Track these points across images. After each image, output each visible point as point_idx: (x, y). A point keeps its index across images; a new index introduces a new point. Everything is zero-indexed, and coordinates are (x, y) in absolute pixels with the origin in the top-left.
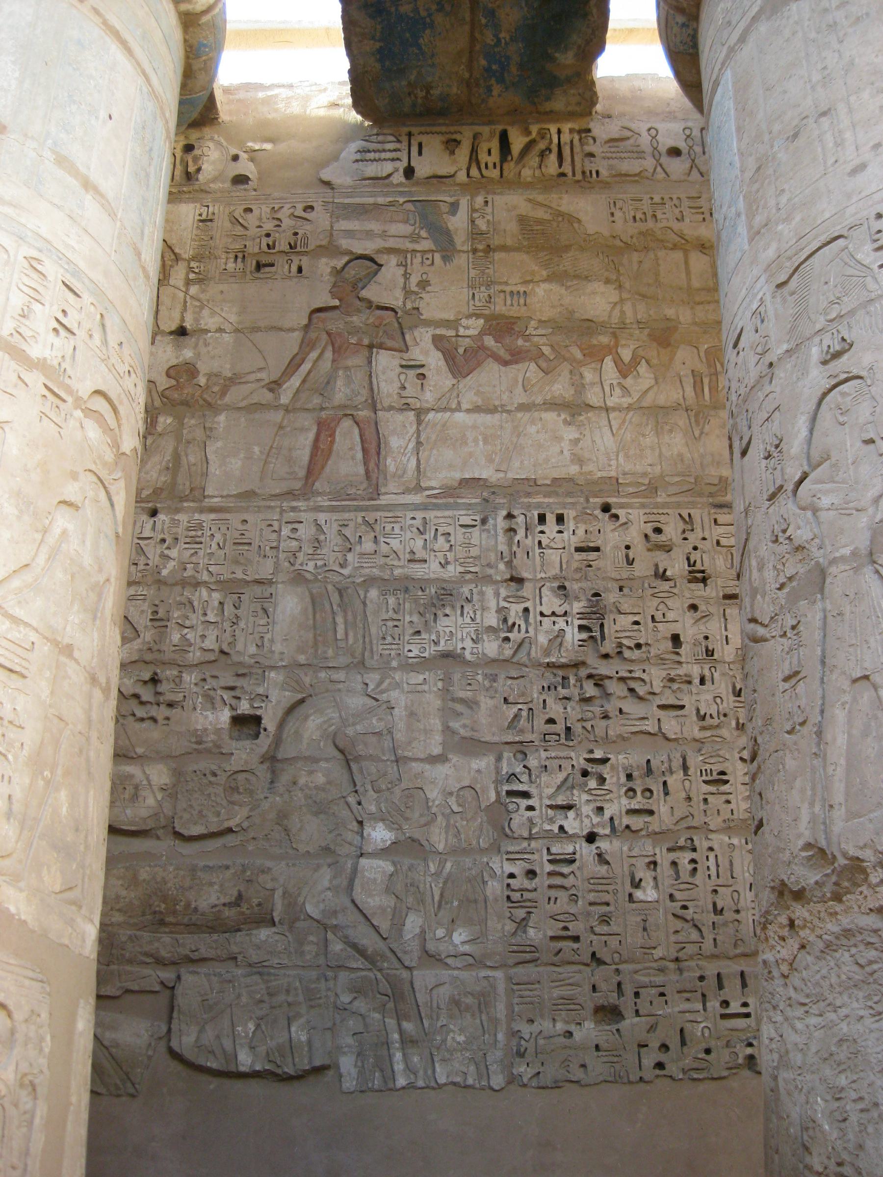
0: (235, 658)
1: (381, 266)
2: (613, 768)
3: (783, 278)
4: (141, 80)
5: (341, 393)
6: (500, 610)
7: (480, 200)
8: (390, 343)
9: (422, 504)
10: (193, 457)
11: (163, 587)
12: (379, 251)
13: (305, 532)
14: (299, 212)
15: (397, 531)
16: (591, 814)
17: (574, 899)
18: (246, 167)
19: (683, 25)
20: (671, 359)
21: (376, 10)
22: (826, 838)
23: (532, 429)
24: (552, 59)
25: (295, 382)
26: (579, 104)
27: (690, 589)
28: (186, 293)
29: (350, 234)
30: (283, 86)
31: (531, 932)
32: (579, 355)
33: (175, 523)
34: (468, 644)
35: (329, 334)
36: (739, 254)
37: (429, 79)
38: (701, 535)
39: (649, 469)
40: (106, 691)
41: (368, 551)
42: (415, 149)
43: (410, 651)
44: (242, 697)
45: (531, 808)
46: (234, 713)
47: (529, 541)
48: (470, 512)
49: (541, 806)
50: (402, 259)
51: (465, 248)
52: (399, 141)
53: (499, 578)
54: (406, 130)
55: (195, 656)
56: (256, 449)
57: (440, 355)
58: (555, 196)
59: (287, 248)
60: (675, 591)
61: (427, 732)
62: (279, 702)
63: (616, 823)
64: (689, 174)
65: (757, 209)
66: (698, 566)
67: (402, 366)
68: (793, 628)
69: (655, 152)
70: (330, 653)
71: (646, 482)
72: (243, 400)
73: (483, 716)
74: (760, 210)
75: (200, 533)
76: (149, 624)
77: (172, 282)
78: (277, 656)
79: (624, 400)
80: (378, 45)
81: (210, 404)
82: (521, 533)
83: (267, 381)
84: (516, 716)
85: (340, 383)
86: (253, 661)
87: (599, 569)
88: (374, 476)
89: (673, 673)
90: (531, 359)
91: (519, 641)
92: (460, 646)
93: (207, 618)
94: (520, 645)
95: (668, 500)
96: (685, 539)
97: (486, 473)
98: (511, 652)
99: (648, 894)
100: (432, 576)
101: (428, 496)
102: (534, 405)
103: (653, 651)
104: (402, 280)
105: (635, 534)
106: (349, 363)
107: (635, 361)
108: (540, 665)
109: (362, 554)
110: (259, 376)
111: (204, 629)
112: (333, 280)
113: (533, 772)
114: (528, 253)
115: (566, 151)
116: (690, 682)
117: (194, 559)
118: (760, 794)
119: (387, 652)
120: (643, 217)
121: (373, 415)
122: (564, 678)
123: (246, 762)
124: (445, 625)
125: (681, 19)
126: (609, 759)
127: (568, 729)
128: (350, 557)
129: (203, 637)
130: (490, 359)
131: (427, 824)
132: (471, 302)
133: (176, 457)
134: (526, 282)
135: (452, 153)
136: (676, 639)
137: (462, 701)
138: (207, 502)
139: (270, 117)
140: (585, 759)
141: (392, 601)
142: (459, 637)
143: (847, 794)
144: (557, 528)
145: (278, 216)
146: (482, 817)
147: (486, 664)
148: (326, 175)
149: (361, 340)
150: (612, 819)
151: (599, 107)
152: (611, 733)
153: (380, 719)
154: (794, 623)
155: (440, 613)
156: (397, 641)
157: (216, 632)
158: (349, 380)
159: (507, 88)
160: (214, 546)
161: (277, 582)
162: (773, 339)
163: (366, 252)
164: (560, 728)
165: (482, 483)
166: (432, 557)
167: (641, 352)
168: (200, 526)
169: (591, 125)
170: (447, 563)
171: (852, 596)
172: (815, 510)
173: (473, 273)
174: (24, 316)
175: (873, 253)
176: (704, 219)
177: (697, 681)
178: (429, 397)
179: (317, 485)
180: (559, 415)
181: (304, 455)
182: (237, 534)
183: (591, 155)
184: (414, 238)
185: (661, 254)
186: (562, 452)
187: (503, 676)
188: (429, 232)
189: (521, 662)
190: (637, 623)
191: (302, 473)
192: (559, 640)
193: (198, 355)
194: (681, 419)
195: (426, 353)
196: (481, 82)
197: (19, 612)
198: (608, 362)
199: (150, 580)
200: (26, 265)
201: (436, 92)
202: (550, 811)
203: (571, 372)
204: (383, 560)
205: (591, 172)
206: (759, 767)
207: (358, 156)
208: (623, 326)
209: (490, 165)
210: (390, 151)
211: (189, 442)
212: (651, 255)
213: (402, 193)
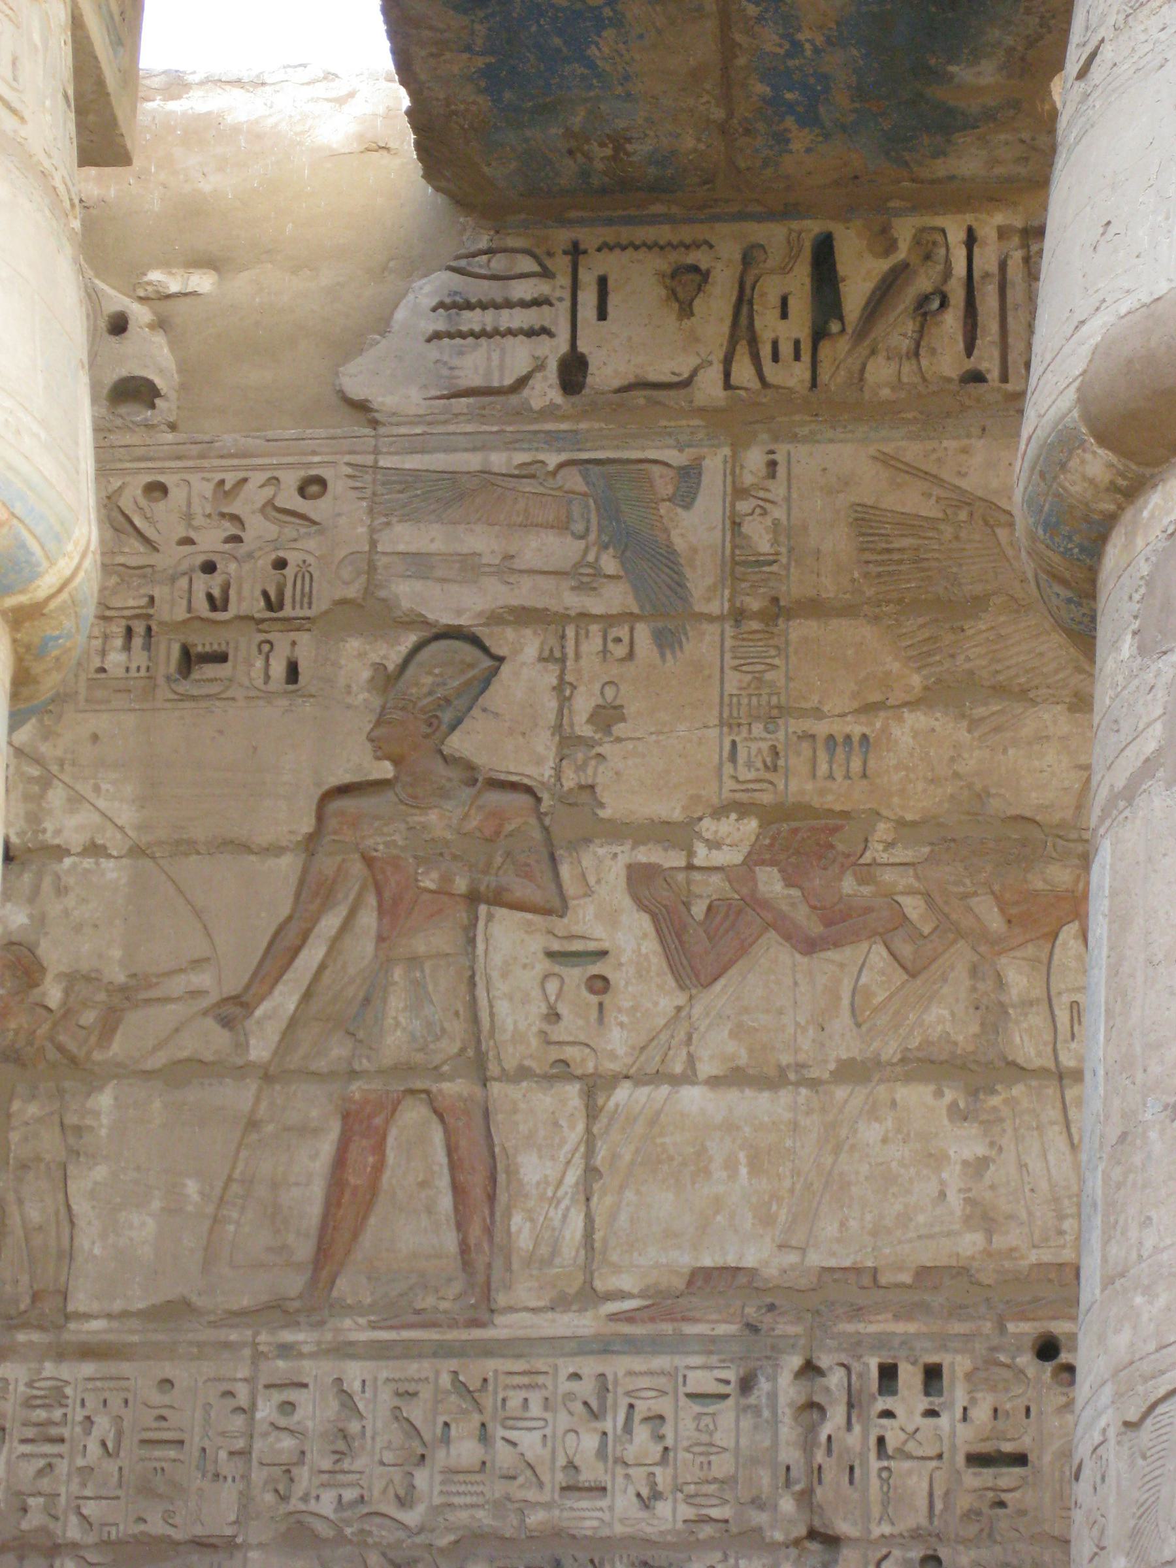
1: (501, 660)
7: (755, 459)
8: (521, 890)
9: (597, 1337)
12: (495, 618)
14: (290, 499)
15: (535, 1409)
23: (870, 1133)
30: (238, 83)
32: (995, 922)
35: (369, 861)
37: (621, 124)
42: (588, 299)
47: (853, 1440)
48: (713, 1360)
50: (553, 641)
51: (714, 608)
52: (546, 274)
53: (779, 1536)
54: (563, 236)
56: (192, 1188)
57: (645, 922)
58: (951, 444)
59: (258, 607)
67: (551, 955)
72: (157, 1048)
75: (57, 1414)
80: (480, 62)
81: (73, 1060)
85: (396, 1003)
87: (1022, 1513)
88: (480, 1261)
100: (619, 1529)
101: (613, 1317)
102: (878, 1064)
104: (554, 704)
109: (451, 1472)
112: (376, 702)
114: (876, 618)
115: (988, 302)
117: (45, 1484)
121: (478, 1090)
128: (421, 1478)
130: (772, 934)
132: (728, 769)
134: (870, 709)
135: (686, 310)
138: (79, 1331)
139: (206, 186)
144: (923, 1403)
145: (235, 508)
149: (447, 879)
160: (94, 1449)
161: (244, 1546)
163: (462, 621)
165: (742, 1280)
166: (620, 1480)
168: (57, 1397)
170: (656, 1495)
179: (343, 1285)
180: (939, 1094)
186: (943, 1195)
188: (622, 558)
191: (304, 1250)
195: (612, 918)
201: (640, 149)
203: (974, 971)
204: (499, 1489)
209: (786, 349)
210: (524, 304)
211: (24, 1167)
213: (553, 440)
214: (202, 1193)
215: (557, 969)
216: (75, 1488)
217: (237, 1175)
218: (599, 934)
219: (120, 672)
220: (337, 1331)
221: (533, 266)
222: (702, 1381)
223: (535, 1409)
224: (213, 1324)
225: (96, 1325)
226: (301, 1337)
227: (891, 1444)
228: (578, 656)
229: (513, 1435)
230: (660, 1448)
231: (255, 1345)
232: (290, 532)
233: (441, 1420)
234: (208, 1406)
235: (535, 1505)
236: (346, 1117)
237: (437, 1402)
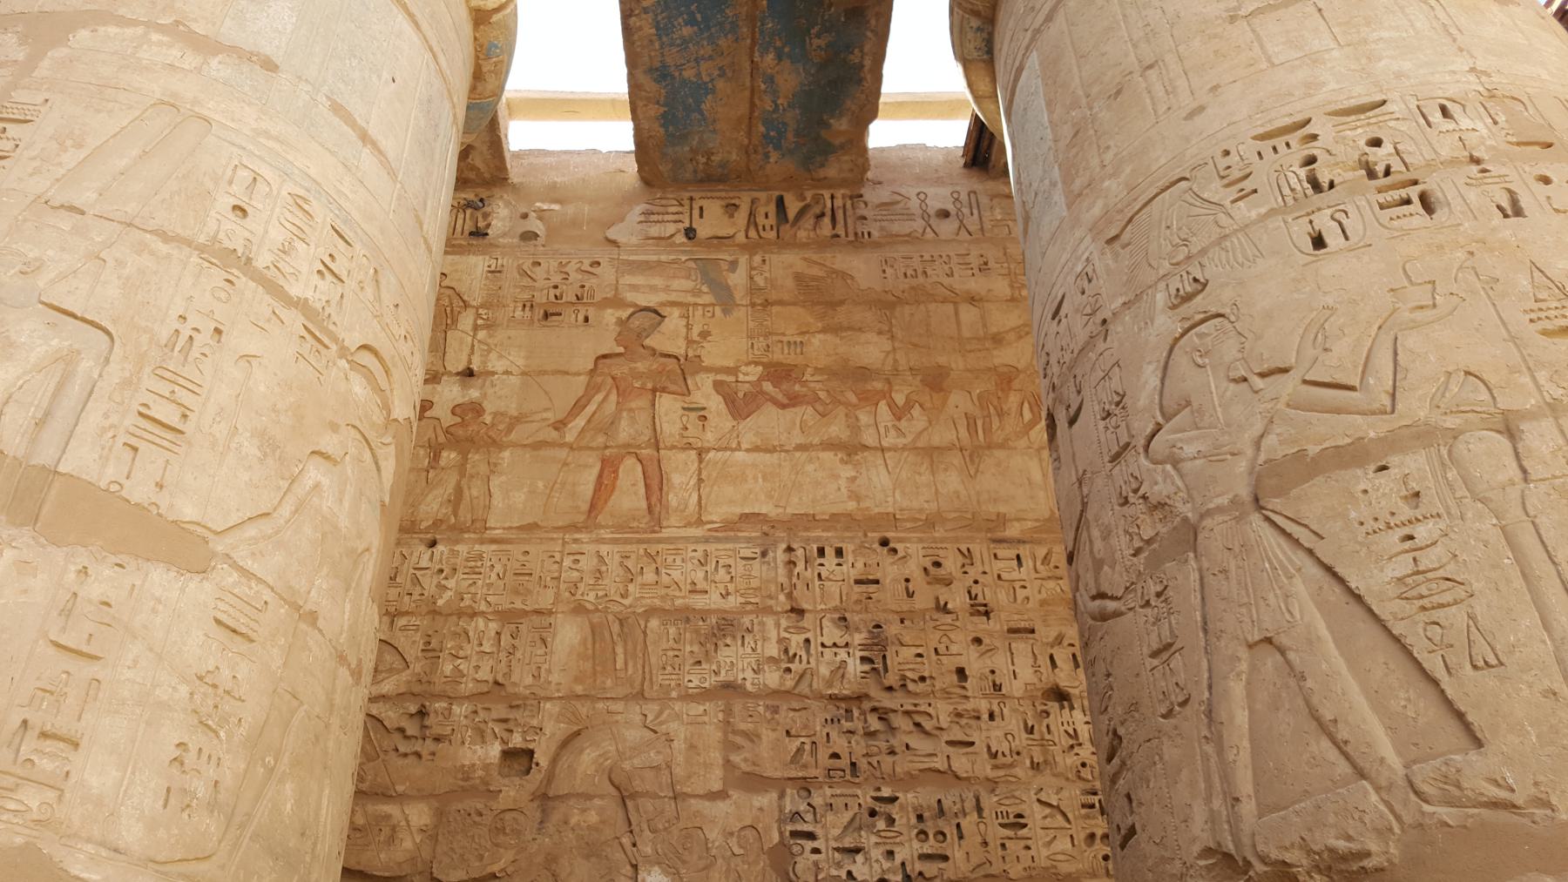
0: (510, 689)
1: (665, 317)
2: (902, 807)
3: (1113, 233)
4: (428, 55)
5: (625, 432)
6: (780, 641)
9: (703, 537)
10: (474, 491)
11: (437, 617)
12: (663, 304)
13: (587, 563)
15: (678, 562)
16: (880, 857)
18: (535, 225)
19: (978, 29)
20: (944, 403)
21: (662, 74)
22: (1233, 841)
23: (810, 468)
24: (827, 126)
25: (580, 422)
26: (851, 170)
27: (972, 622)
28: (474, 337)
29: (634, 288)
32: (853, 398)
33: (454, 553)
34: (749, 674)
35: (613, 378)
36: (1056, 223)
37: (711, 145)
38: (981, 569)
39: (926, 505)
40: (357, 674)
41: (649, 581)
42: (696, 212)
43: (690, 681)
44: (515, 730)
45: (816, 851)
46: (506, 748)
48: (750, 545)
49: (827, 849)
51: (744, 303)
52: (681, 205)
53: (779, 609)
54: (688, 195)
55: (468, 687)
57: (720, 398)
58: (829, 255)
60: (958, 624)
61: (707, 766)
62: (553, 734)
63: (908, 869)
64: (958, 234)
65: (1077, 172)
66: (980, 599)
67: (684, 409)
68: (1159, 595)
69: (925, 216)
70: (609, 683)
71: (924, 518)
73: (764, 749)
74: (1081, 172)
75: (479, 564)
76: (420, 654)
77: (460, 326)
78: (553, 687)
79: (898, 440)
80: (662, 109)
81: (494, 441)
83: (552, 421)
84: (798, 750)
86: (528, 692)
87: (879, 601)
88: (657, 509)
89: (960, 708)
90: (808, 403)
91: (801, 672)
92: (741, 676)
93: (482, 649)
94: (802, 676)
95: (946, 535)
96: (966, 573)
97: (763, 508)
98: (793, 683)
100: (713, 606)
101: (709, 530)
102: (812, 445)
103: (938, 685)
104: (685, 330)
105: (913, 567)
106: (633, 405)
107: (909, 405)
108: (822, 697)
110: (545, 415)
111: (477, 661)
112: (618, 329)
113: (817, 810)
114: (804, 306)
115: (840, 215)
116: (978, 718)
117: (473, 590)
118: (1128, 797)
119: (667, 682)
120: (913, 273)
121: (656, 453)
122: (847, 711)
123: (515, 800)
124: (726, 655)
125: (975, 23)
126: (897, 798)
127: (853, 764)
128: (631, 587)
129: (477, 667)
130: (769, 403)
131: (706, 868)
133: (459, 491)
134: (803, 333)
135: (732, 216)
136: (961, 672)
137: (745, 734)
140: (873, 798)
141: (672, 630)
142: (740, 667)
143: (1256, 784)
144: (836, 561)
146: (763, 862)
147: (767, 695)
148: (612, 234)
150: (903, 864)
151: (869, 175)
152: (898, 769)
153: (659, 752)
154: (1159, 588)
155: (720, 643)
156: (677, 671)
157: (491, 662)
158: (633, 420)
159: (783, 155)
160: (494, 576)
162: (1104, 296)
164: (844, 763)
167: (914, 397)
168: (481, 558)
169: (863, 191)
170: (728, 594)
171: (1237, 549)
172: (1176, 462)
173: (751, 324)
174: (284, 252)
175: (1222, 189)
176: (973, 275)
177: (986, 716)
178: (710, 437)
181: (587, 489)
182: (517, 565)
183: (865, 218)
184: (697, 292)
185: (932, 306)
186: (839, 489)
187: (785, 708)
188: (709, 287)
189: (804, 693)
190: (920, 655)
191: (585, 507)
192: (841, 671)
193: (485, 395)
194: (956, 459)
196: (760, 148)
197: (248, 564)
198: (883, 406)
199: (424, 609)
200: (291, 201)
202: (836, 854)
203: (847, 415)
204: (663, 592)
205: (863, 233)
206: (1123, 763)
207: (642, 218)
208: (896, 371)
209: (768, 228)
212: (922, 307)
213: (684, 252)
214: (544, 486)
215: (686, 413)
216: (485, 591)
217: (559, 481)
218: (703, 402)
219: (520, 318)
220: (598, 534)
221: (676, 203)
222: (747, 553)
223: (678, 562)
224: (546, 532)
225: (497, 531)
226: (583, 536)
227: (823, 576)
228: (694, 316)
229: (668, 571)
230: (729, 576)
231: (563, 539)
232: (586, 277)
233: (639, 566)
234: (543, 561)
235: (678, 597)
236: (602, 462)
237: (638, 559)
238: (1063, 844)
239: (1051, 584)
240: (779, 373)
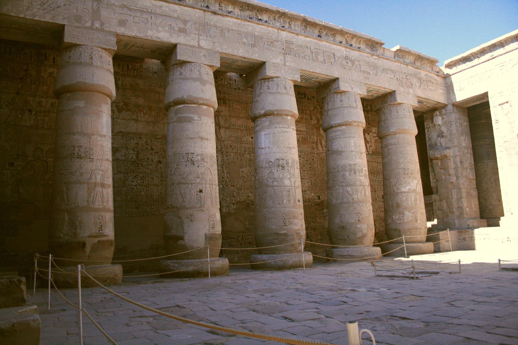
6: (125, 152)
7: (123, 78)
17: (133, 194)
23: (130, 123)
31: (128, 198)
32: (138, 111)
82: (128, 141)
99: (143, 193)
115: (138, 70)
135: (119, 67)
136: (148, 158)
164: (132, 170)
183: (142, 71)
198: (142, 113)
222: (120, 138)
238: (158, 181)
239: (162, 146)
240: (126, 104)
